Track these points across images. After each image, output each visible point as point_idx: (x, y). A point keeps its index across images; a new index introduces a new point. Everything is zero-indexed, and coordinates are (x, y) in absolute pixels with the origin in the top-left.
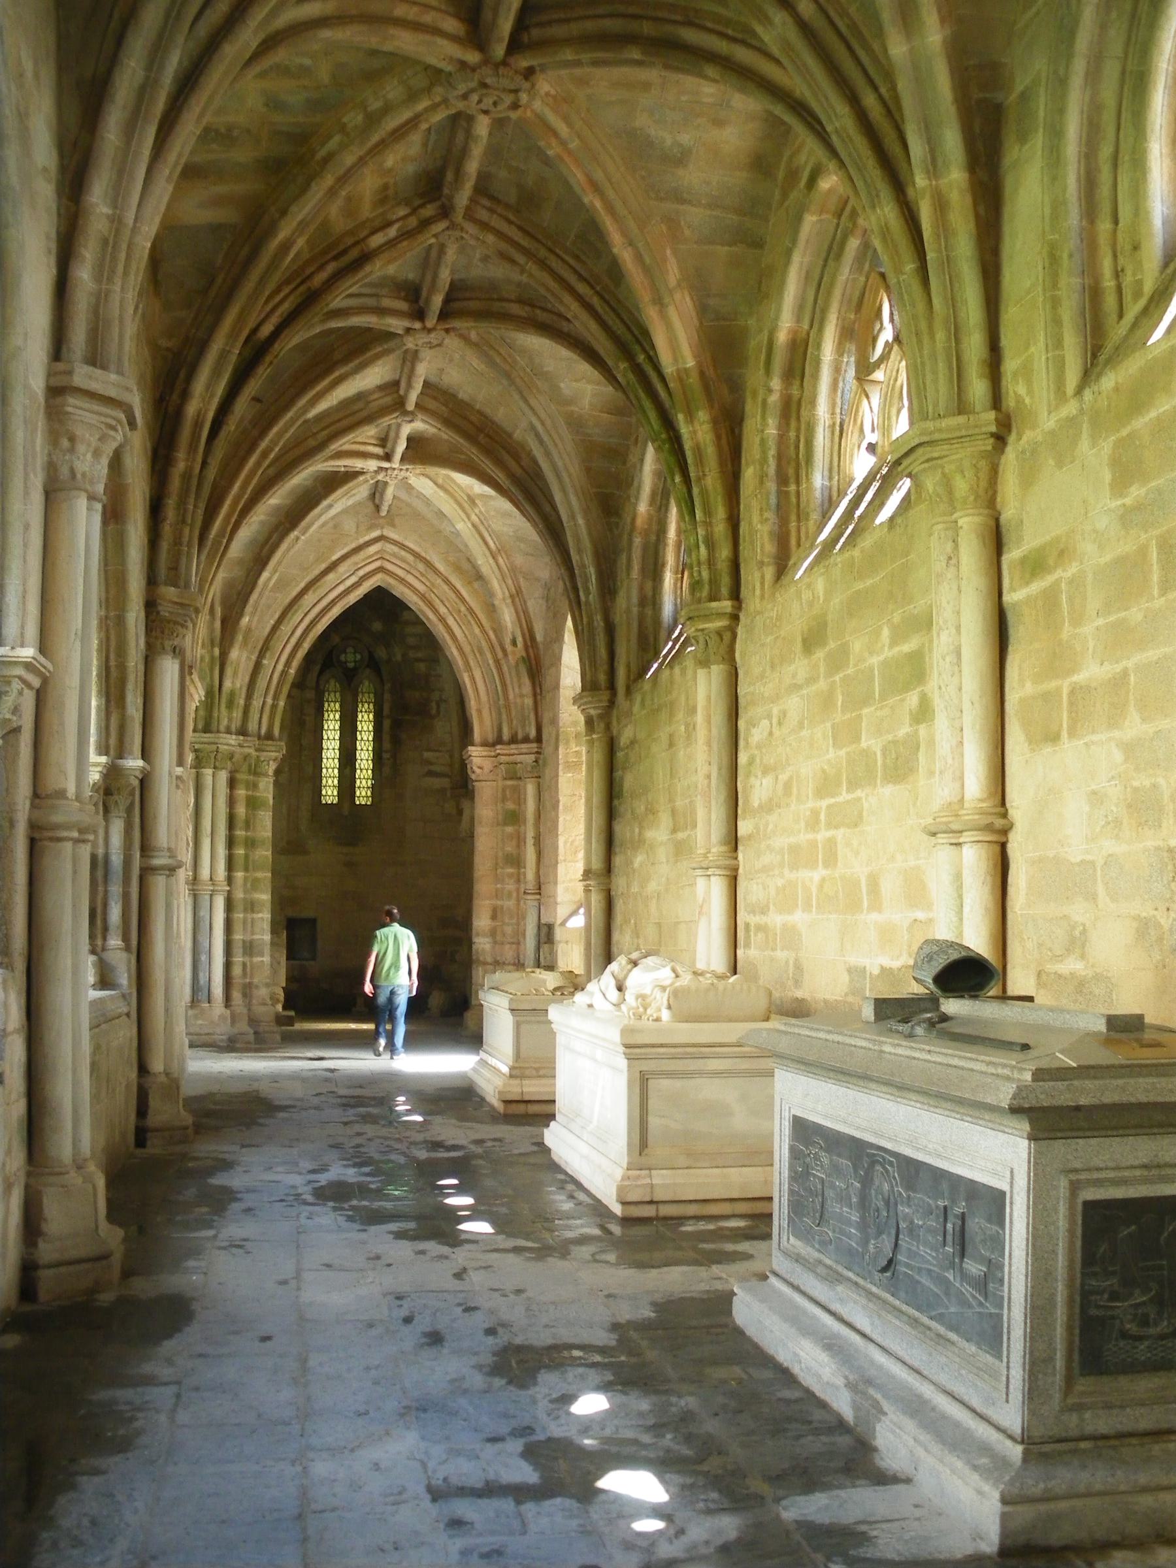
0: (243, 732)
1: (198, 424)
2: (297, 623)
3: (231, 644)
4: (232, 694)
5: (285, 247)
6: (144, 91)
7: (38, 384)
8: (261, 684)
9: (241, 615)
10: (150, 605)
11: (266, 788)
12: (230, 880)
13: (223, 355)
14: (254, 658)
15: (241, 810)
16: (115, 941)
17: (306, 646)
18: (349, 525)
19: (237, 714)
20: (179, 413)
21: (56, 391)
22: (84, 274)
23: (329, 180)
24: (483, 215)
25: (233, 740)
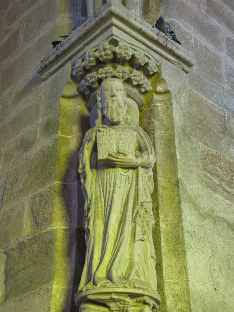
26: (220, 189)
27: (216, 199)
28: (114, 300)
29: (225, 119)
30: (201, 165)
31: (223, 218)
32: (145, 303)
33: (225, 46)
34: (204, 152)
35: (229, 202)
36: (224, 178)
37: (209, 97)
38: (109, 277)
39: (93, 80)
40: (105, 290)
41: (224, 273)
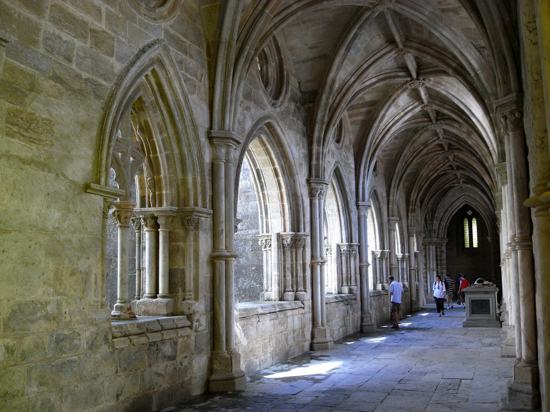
0: (438, 237)
1: (413, 201)
3: (434, 220)
4: (435, 230)
5: (423, 174)
6: (395, 184)
7: (386, 220)
8: (441, 227)
9: (435, 214)
10: (408, 230)
11: (444, 248)
12: (437, 268)
13: (415, 190)
14: (439, 222)
15: (439, 253)
16: (405, 280)
17: (450, 219)
19: (436, 234)
20: (410, 200)
21: (389, 220)
22: (390, 206)
23: (427, 165)
24: (456, 160)
25: (436, 239)
26: (18, 135)
27: (13, 143)
29: (35, 78)
30: (4, 120)
31: (16, 156)
33: (49, 13)
34: (8, 109)
35: (24, 143)
36: (23, 126)
37: (22, 63)
41: (9, 192)
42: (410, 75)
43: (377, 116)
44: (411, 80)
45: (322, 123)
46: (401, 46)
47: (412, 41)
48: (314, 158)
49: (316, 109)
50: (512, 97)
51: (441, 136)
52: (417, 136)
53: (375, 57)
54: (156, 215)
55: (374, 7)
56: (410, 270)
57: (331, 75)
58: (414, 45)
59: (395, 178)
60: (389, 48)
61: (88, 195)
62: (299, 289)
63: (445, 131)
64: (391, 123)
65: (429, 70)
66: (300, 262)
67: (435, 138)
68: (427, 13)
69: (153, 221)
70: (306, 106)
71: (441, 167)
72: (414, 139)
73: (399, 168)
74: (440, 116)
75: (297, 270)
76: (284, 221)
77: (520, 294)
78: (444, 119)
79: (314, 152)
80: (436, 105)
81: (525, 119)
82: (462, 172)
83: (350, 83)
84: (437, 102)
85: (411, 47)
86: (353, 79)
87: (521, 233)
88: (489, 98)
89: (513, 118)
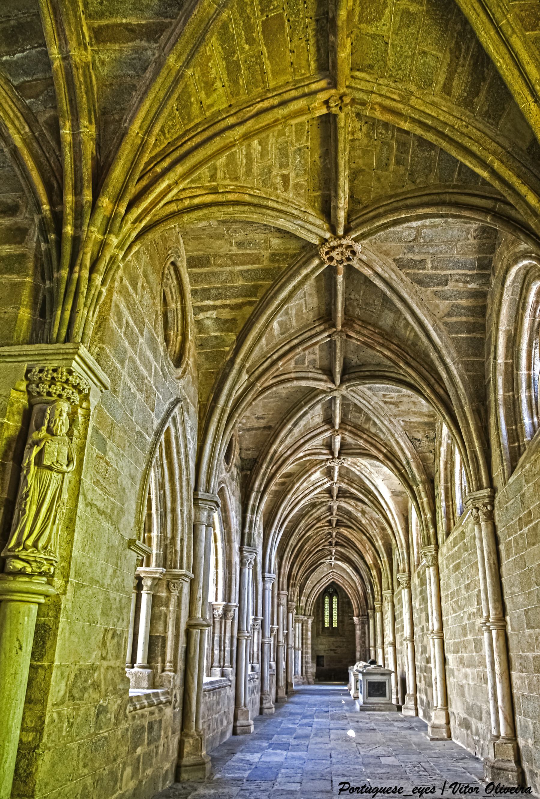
0: (304, 615)
2: (316, 590)
8: (308, 604)
12: (302, 647)
15: (304, 632)
18: (325, 569)
21: (279, 594)
22: (281, 580)
25: (302, 616)
28: (36, 561)
32: (52, 564)
38: (35, 545)
39: (45, 390)
40: (33, 555)
42: (332, 453)
43: (292, 488)
44: (332, 459)
45: (258, 492)
46: (337, 427)
47: (347, 424)
48: (247, 525)
49: (254, 476)
50: (486, 492)
51: (335, 513)
52: (314, 511)
53: (312, 434)
54: (142, 576)
55: (331, 392)
56: (287, 648)
57: (274, 447)
58: (349, 428)
59: (288, 550)
60: (325, 428)
61: (130, 550)
62: (226, 664)
63: (339, 508)
64: (301, 496)
65: (351, 451)
66: (228, 635)
67: (328, 514)
68: (372, 403)
69: (137, 581)
70: (244, 473)
71: (323, 542)
72: (311, 513)
73: (293, 541)
74: (343, 494)
75: (225, 643)
76: (217, 589)
77: (497, 672)
78: (345, 497)
79: (248, 520)
80: (344, 483)
81: (496, 512)
82: (339, 549)
83: (286, 455)
84: (346, 481)
85: (346, 430)
86: (289, 452)
87: (496, 614)
88: (417, 486)
89: (485, 510)
